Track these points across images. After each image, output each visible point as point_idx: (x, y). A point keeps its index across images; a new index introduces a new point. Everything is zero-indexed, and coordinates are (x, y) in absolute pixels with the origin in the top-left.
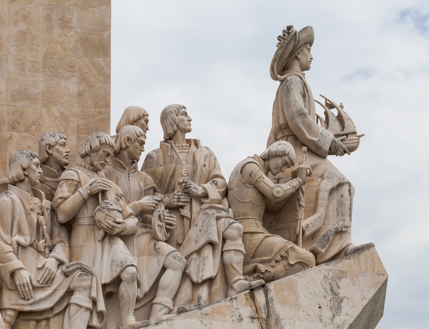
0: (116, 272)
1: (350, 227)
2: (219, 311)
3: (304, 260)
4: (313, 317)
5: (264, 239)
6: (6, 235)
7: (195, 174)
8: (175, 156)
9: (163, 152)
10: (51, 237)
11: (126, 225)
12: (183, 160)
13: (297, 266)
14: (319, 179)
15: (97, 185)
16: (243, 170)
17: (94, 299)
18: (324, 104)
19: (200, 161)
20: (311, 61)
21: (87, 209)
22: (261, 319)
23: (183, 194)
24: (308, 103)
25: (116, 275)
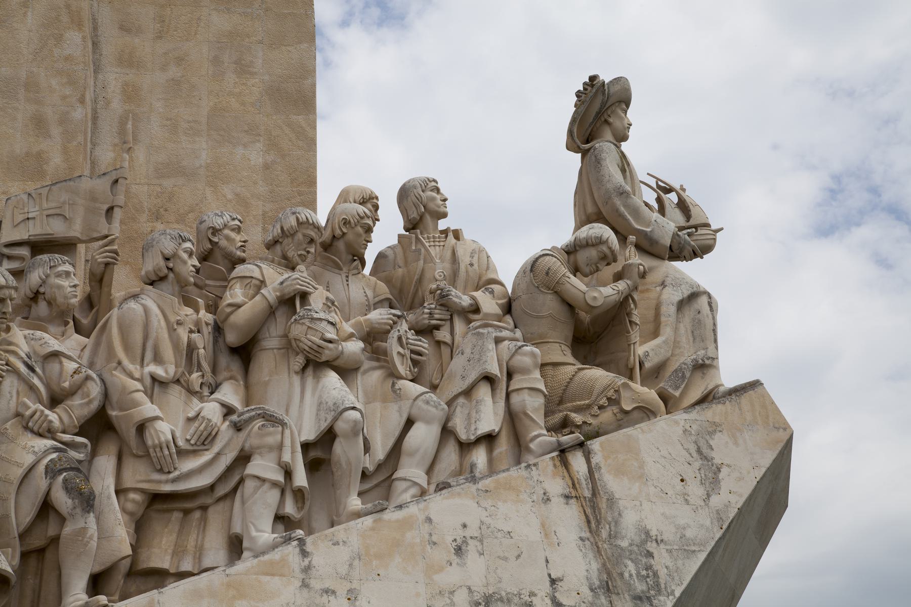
0: (326, 420)
1: (717, 358)
2: (508, 486)
3: (646, 404)
4: (672, 495)
5: (576, 372)
6: (133, 364)
7: (456, 278)
8: (423, 250)
9: (403, 248)
10: (214, 371)
11: (342, 348)
12: (436, 257)
13: (636, 414)
14: (658, 289)
15: (293, 282)
16: (534, 267)
17: (286, 466)
18: (655, 186)
19: (464, 259)
20: (629, 128)
21: (276, 320)
22: (582, 499)
23: (438, 307)
24: (630, 182)
25: (327, 426)
